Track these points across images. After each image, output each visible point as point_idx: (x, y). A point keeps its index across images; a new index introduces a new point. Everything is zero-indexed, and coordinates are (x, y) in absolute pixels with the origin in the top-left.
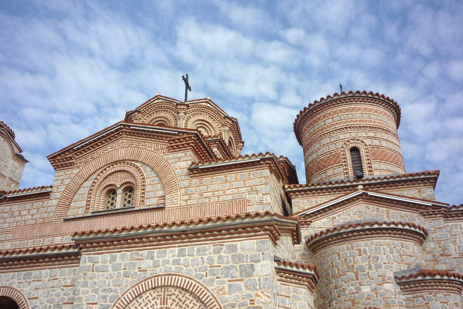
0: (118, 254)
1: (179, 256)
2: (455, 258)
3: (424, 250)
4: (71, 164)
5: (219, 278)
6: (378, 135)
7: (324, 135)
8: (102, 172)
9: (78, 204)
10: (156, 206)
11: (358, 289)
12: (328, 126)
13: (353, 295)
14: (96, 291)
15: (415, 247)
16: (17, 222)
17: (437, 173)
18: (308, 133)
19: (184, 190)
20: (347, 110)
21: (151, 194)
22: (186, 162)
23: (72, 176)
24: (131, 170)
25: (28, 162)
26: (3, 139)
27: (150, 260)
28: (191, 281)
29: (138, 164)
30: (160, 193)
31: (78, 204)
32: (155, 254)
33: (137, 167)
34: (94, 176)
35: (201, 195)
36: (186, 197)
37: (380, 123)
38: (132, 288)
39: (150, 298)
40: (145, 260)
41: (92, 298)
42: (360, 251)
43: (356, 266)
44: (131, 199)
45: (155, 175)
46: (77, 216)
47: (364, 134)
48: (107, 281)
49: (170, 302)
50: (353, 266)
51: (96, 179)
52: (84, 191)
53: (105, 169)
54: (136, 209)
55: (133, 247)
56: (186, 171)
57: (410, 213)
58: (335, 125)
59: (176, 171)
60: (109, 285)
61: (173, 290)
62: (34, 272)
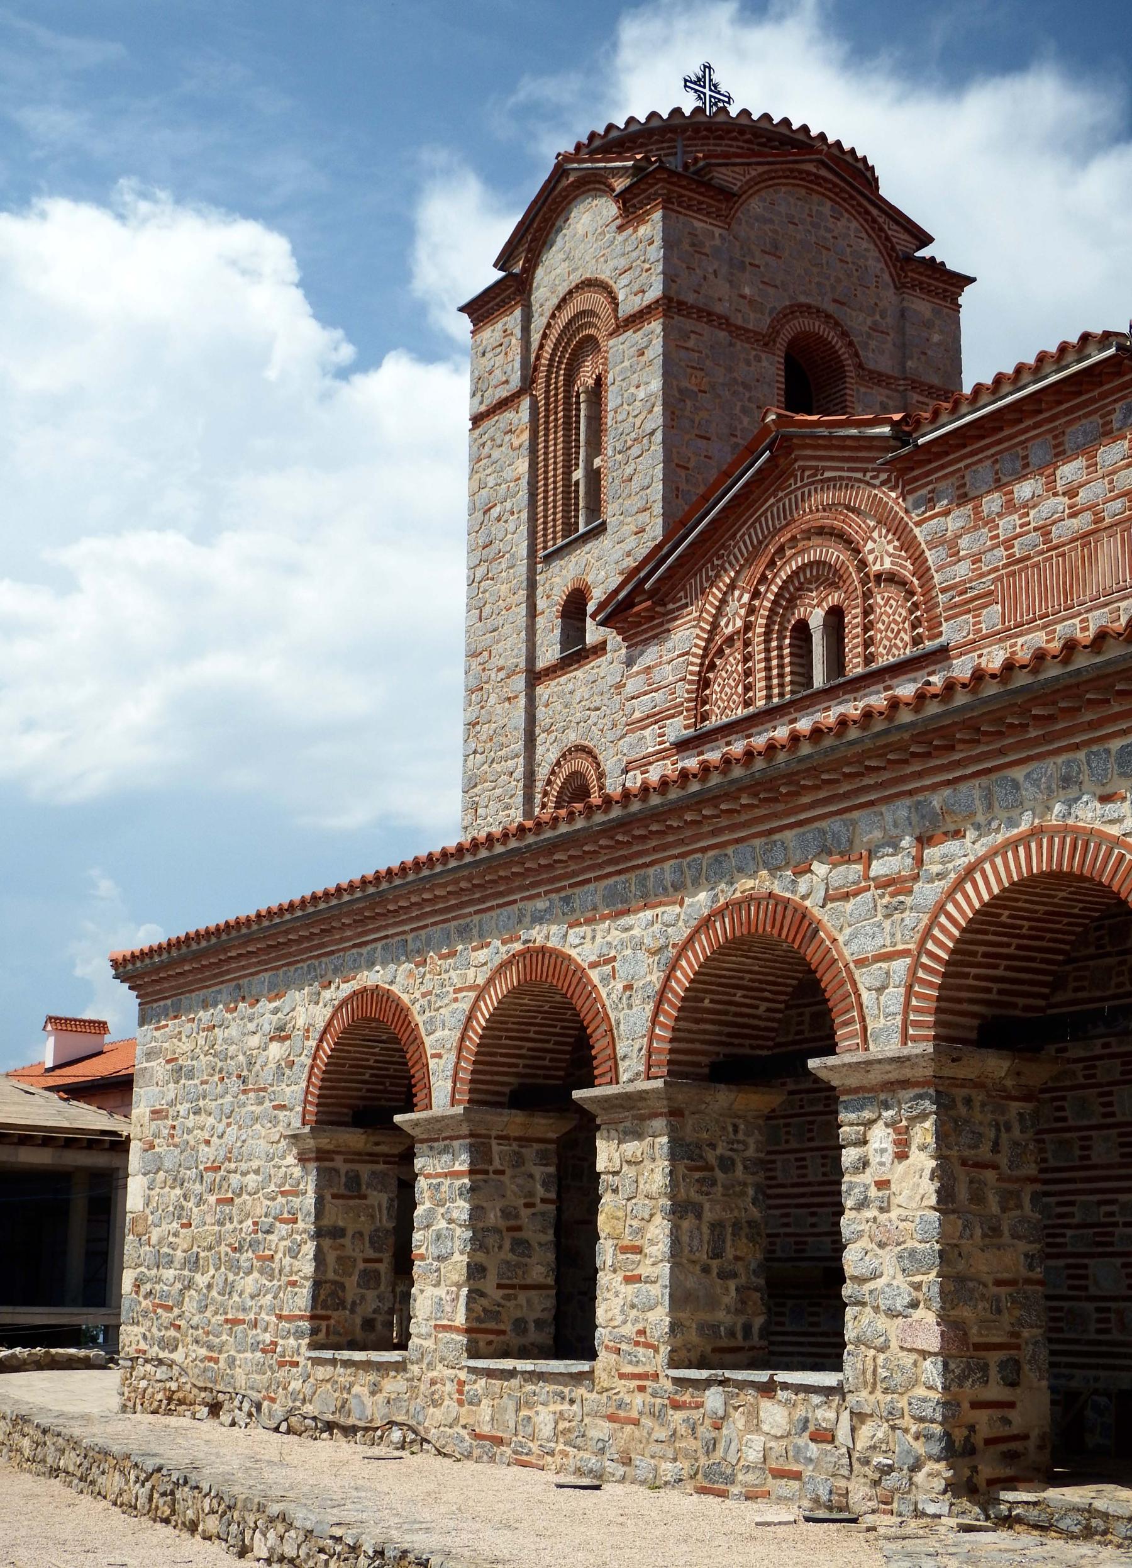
16: (1008, 544)
25: (973, 280)
26: (829, 204)
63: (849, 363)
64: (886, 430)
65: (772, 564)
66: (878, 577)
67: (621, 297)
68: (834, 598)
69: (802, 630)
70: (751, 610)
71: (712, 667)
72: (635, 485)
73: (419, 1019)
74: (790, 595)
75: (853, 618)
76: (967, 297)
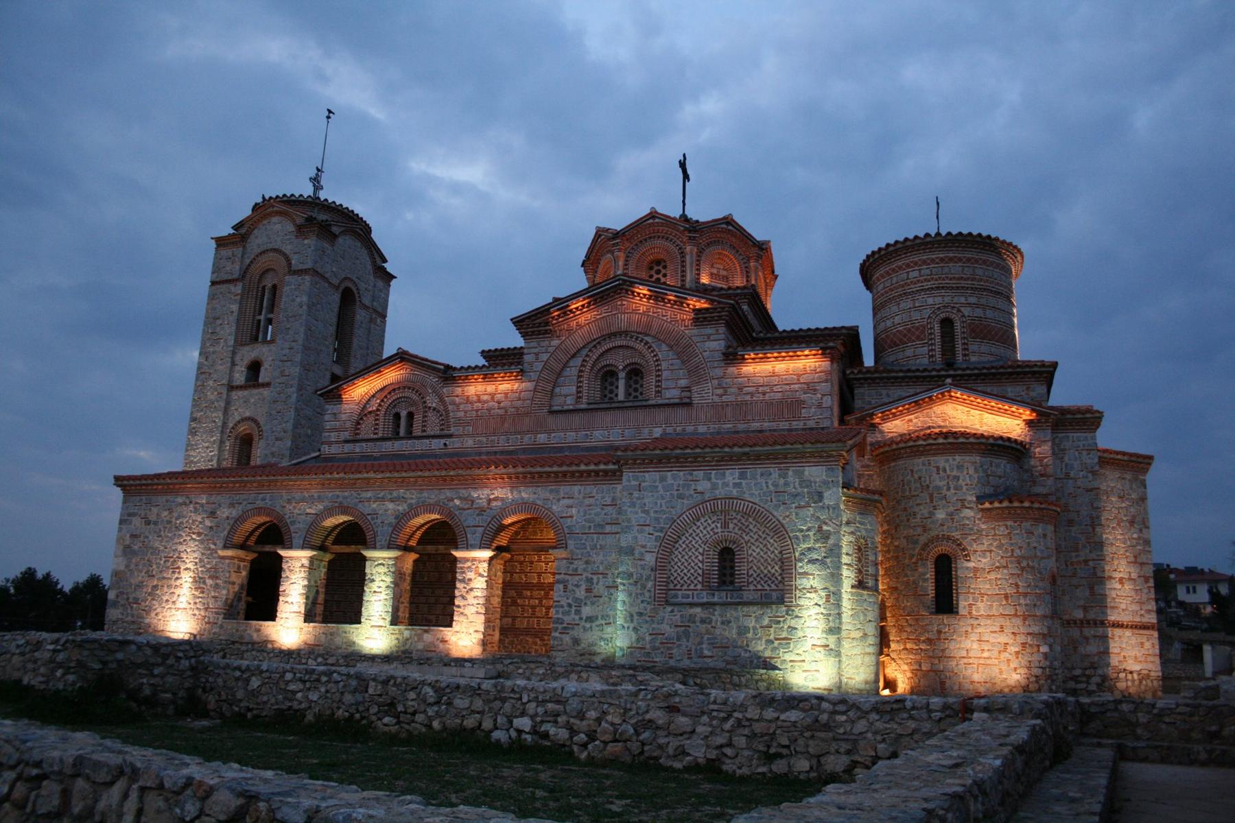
0: (669, 474)
1: (739, 479)
2: (1060, 479)
3: (1021, 468)
4: (546, 332)
5: (786, 504)
6: (983, 301)
7: (905, 293)
8: (595, 346)
9: (565, 390)
10: (677, 401)
11: (931, 514)
12: (911, 282)
13: (925, 521)
14: (647, 512)
15: (1008, 466)
16: (477, 411)
17: (1054, 365)
19: (716, 382)
20: (942, 260)
21: (671, 384)
23: (551, 349)
24: (639, 346)
25: (395, 277)
27: (706, 482)
28: (754, 506)
30: (683, 383)
31: (565, 390)
32: (713, 476)
33: (647, 343)
34: (585, 352)
35: (740, 389)
36: (720, 391)
37: (987, 281)
38: (688, 510)
39: (710, 522)
40: (701, 482)
41: (642, 520)
42: (938, 468)
43: (931, 486)
44: (638, 386)
45: (675, 357)
46: (566, 408)
47: (963, 300)
48: (659, 502)
49: (731, 526)
50: (928, 486)
51: (587, 356)
52: (572, 372)
53: (599, 343)
54: (651, 402)
55: (686, 467)
56: (719, 356)
58: (922, 282)
59: (705, 354)
60: (661, 506)
61: (734, 514)
62: (562, 487)
63: (358, 299)
64: (442, 367)
65: (390, 393)
66: (430, 408)
67: (293, 262)
68: (412, 409)
69: (397, 416)
70: (380, 405)
71: (362, 419)
72: (291, 332)
73: (288, 521)
74: (394, 404)
75: (418, 418)
76: (393, 283)
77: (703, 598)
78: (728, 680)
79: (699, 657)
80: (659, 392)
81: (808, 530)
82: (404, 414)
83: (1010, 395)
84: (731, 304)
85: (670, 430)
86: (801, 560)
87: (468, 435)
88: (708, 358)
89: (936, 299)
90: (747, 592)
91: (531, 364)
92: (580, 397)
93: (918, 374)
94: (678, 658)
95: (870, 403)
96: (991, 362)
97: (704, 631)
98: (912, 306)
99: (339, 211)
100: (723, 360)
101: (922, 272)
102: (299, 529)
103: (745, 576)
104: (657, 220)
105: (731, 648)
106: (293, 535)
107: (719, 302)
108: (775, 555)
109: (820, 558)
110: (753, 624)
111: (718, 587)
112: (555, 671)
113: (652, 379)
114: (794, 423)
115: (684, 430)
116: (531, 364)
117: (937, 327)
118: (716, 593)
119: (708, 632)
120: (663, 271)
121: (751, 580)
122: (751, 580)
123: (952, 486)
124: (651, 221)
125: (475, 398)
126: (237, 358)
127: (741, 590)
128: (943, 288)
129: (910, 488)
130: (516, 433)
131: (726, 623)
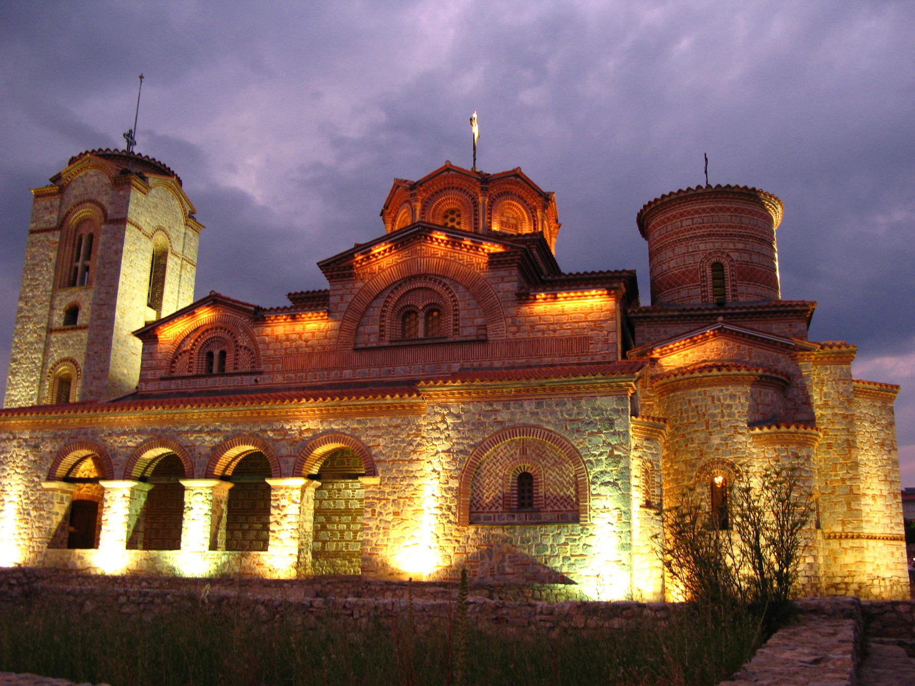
6: (749, 247)
8: (396, 288)
10: (474, 338)
11: (706, 441)
12: (685, 230)
15: (775, 395)
16: (286, 349)
18: (658, 232)
20: (712, 210)
22: (511, 284)
24: (438, 288)
28: (550, 434)
29: (447, 282)
30: (479, 321)
31: (368, 329)
33: (445, 285)
34: (386, 294)
36: (514, 329)
37: (753, 229)
42: (713, 398)
43: (707, 414)
46: (370, 345)
47: (731, 246)
51: (389, 297)
54: (451, 339)
56: (512, 297)
57: (775, 354)
58: (695, 230)
59: (498, 294)
64: (253, 308)
65: (203, 333)
66: (241, 347)
67: (109, 212)
68: (225, 348)
69: (210, 355)
70: (194, 345)
74: (207, 344)
75: (230, 356)
77: (504, 519)
78: (530, 595)
79: (501, 574)
80: (456, 330)
81: (601, 454)
82: (216, 353)
83: (775, 331)
84: (523, 248)
85: (467, 365)
86: (594, 483)
87: (278, 372)
88: (502, 298)
89: (707, 245)
90: (545, 513)
91: (336, 305)
92: (383, 336)
93: (692, 313)
94: (482, 576)
95: (649, 340)
96: (758, 302)
97: (505, 550)
98: (685, 251)
99: (151, 164)
100: (516, 300)
101: (695, 220)
102: (120, 460)
103: (543, 498)
104: (451, 173)
105: (531, 566)
106: (114, 467)
107: (512, 247)
108: (570, 478)
109: (612, 481)
110: (551, 542)
111: (518, 509)
112: (370, 590)
113: (451, 318)
114: (582, 358)
115: (480, 365)
116: (336, 305)
117: (709, 271)
118: (516, 515)
119: (509, 550)
120: (457, 220)
121: (548, 502)
122: (548, 502)
123: (726, 414)
124: (446, 173)
125: (284, 338)
126: (57, 302)
127: (539, 511)
128: (713, 235)
129: (688, 416)
130: (322, 369)
131: (525, 541)
